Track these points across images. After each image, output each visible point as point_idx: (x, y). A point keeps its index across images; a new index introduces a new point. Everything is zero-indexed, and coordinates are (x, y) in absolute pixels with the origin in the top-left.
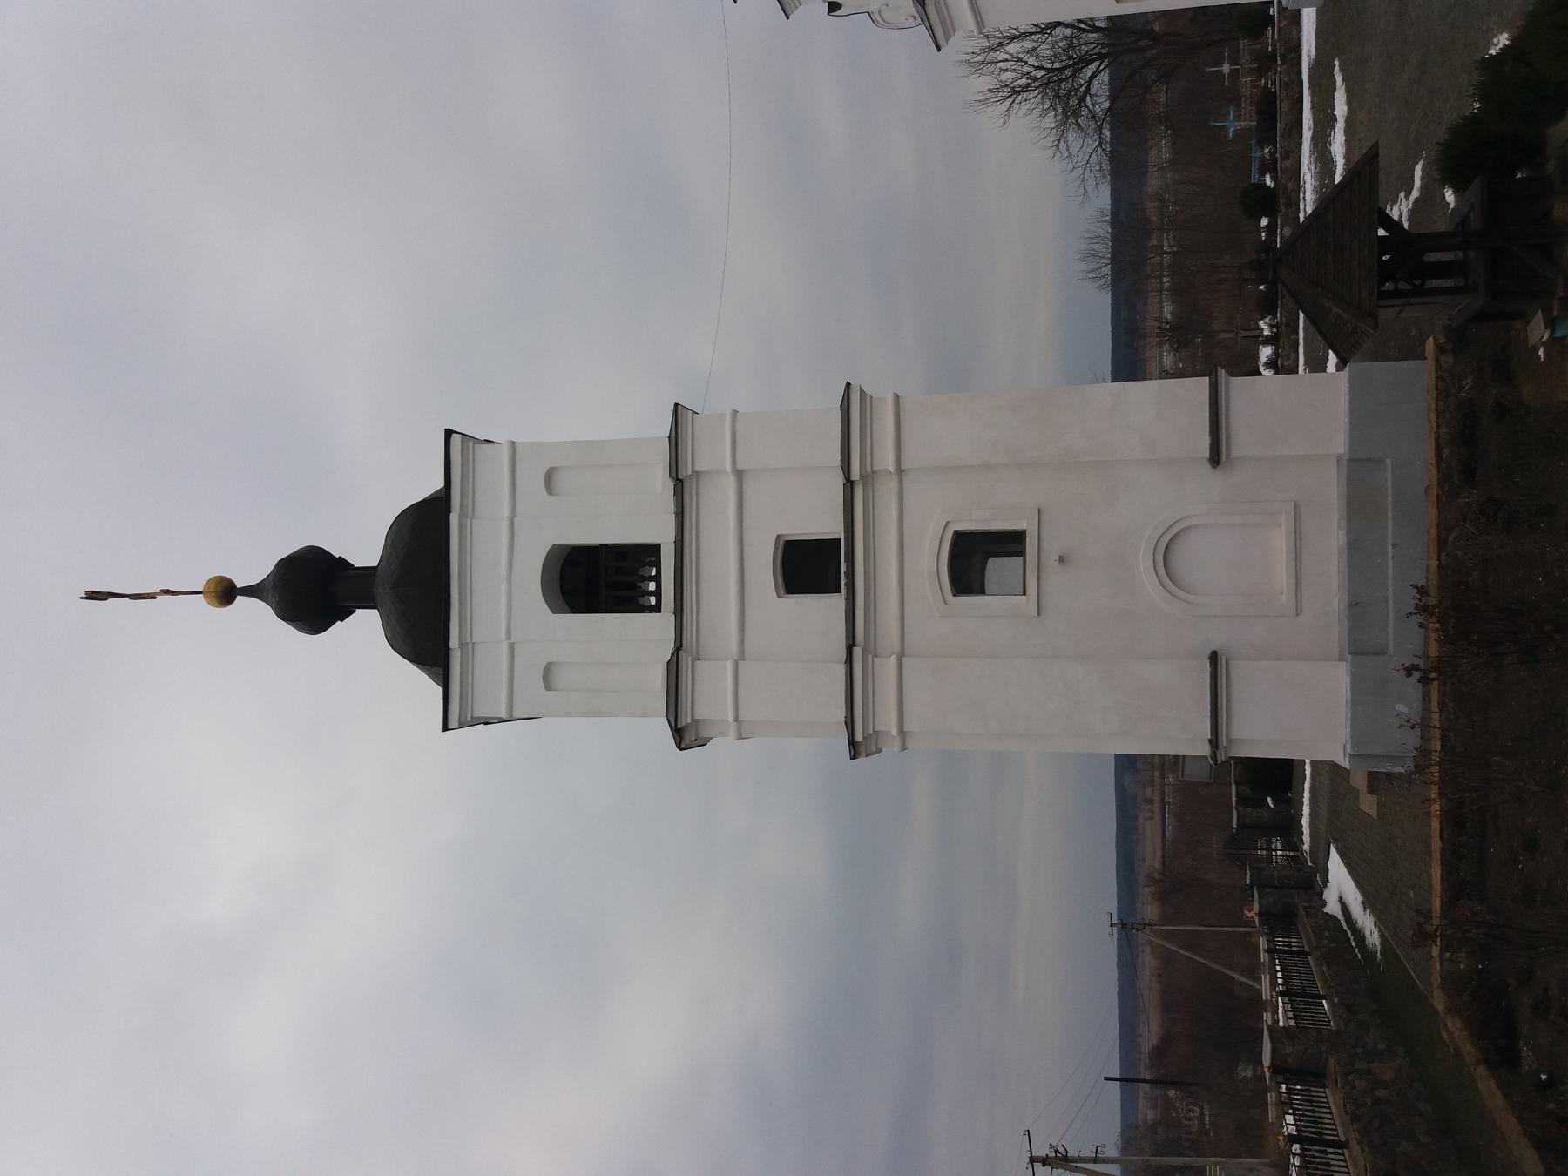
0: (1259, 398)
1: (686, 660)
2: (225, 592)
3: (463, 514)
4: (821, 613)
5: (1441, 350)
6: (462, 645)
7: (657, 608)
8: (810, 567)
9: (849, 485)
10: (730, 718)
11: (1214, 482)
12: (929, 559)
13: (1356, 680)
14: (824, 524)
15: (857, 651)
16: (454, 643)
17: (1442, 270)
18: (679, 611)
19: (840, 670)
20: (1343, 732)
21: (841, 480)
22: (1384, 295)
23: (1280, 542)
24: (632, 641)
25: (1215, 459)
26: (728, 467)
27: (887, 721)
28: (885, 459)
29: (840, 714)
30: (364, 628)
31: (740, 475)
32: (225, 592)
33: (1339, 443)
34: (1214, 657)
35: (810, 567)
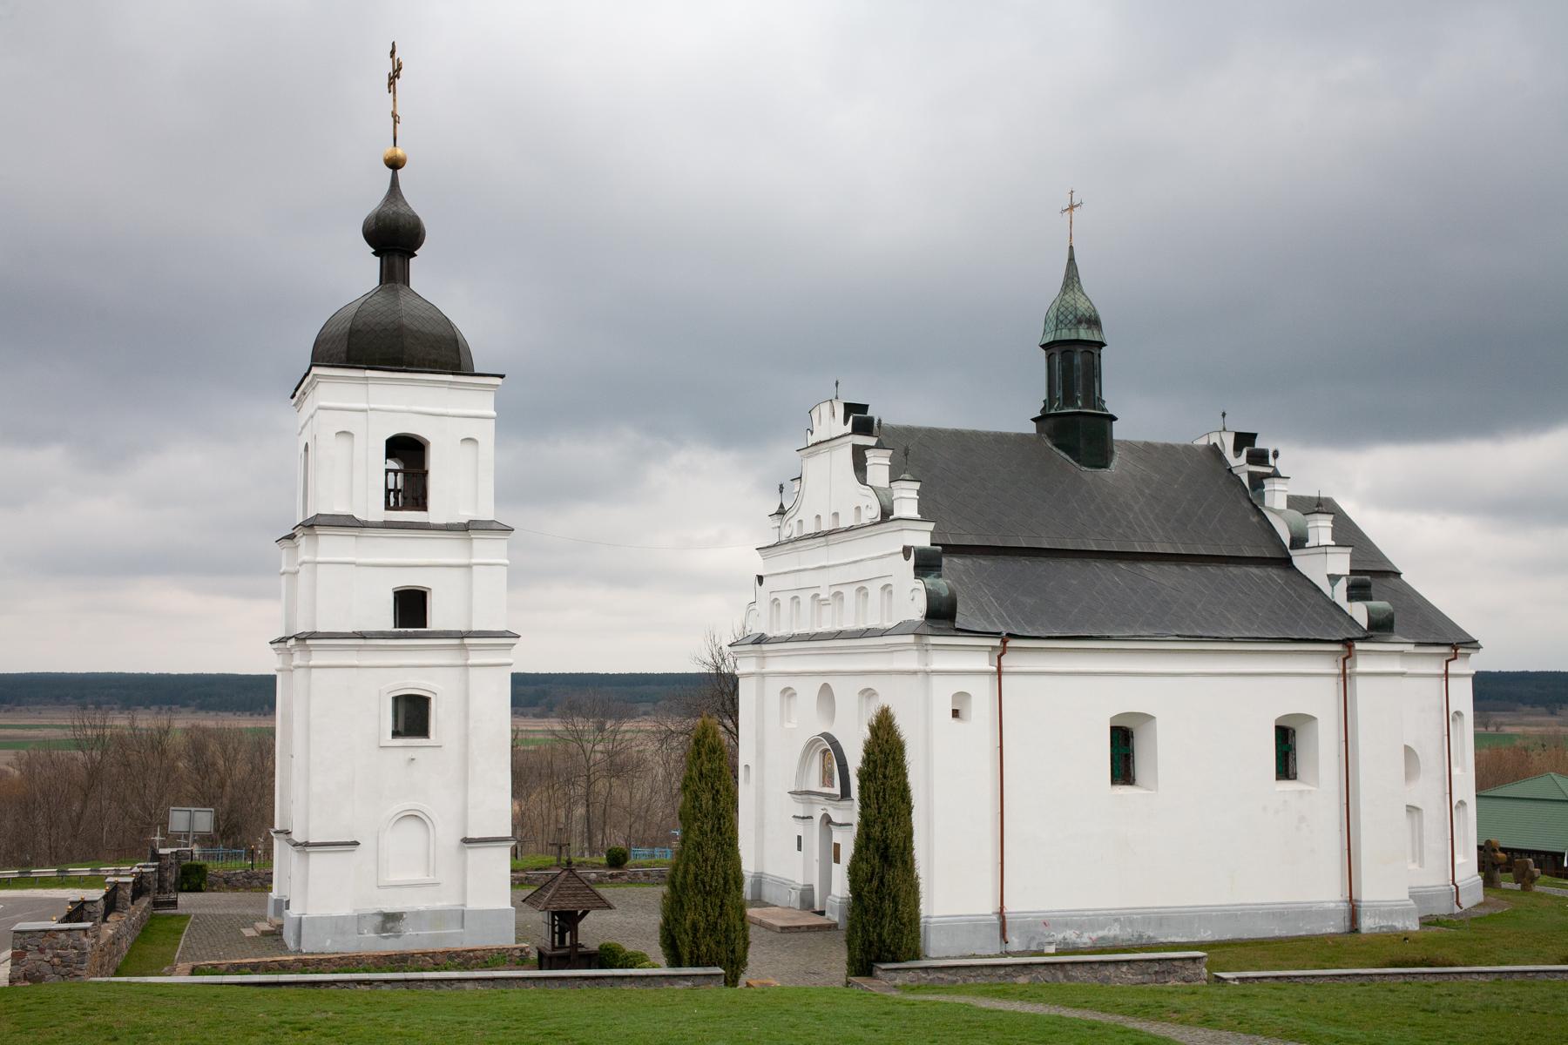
0: (499, 863)
1: (356, 532)
2: (395, 164)
3: (451, 383)
5: (522, 950)
6: (367, 378)
7: (388, 507)
8: (411, 607)
9: (462, 635)
10: (319, 559)
11: (455, 840)
12: (413, 684)
13: (344, 918)
14: (437, 617)
15: (362, 642)
16: (369, 373)
17: (562, 940)
18: (388, 525)
19: (349, 630)
20: (313, 912)
21: (463, 629)
22: (554, 914)
23: (419, 876)
24: (363, 483)
25: (466, 841)
26: (474, 561)
27: (318, 658)
28: (475, 658)
29: (320, 629)
30: (365, 270)
31: (469, 566)
32: (395, 164)
33: (472, 905)
34: (356, 843)
35: (411, 607)
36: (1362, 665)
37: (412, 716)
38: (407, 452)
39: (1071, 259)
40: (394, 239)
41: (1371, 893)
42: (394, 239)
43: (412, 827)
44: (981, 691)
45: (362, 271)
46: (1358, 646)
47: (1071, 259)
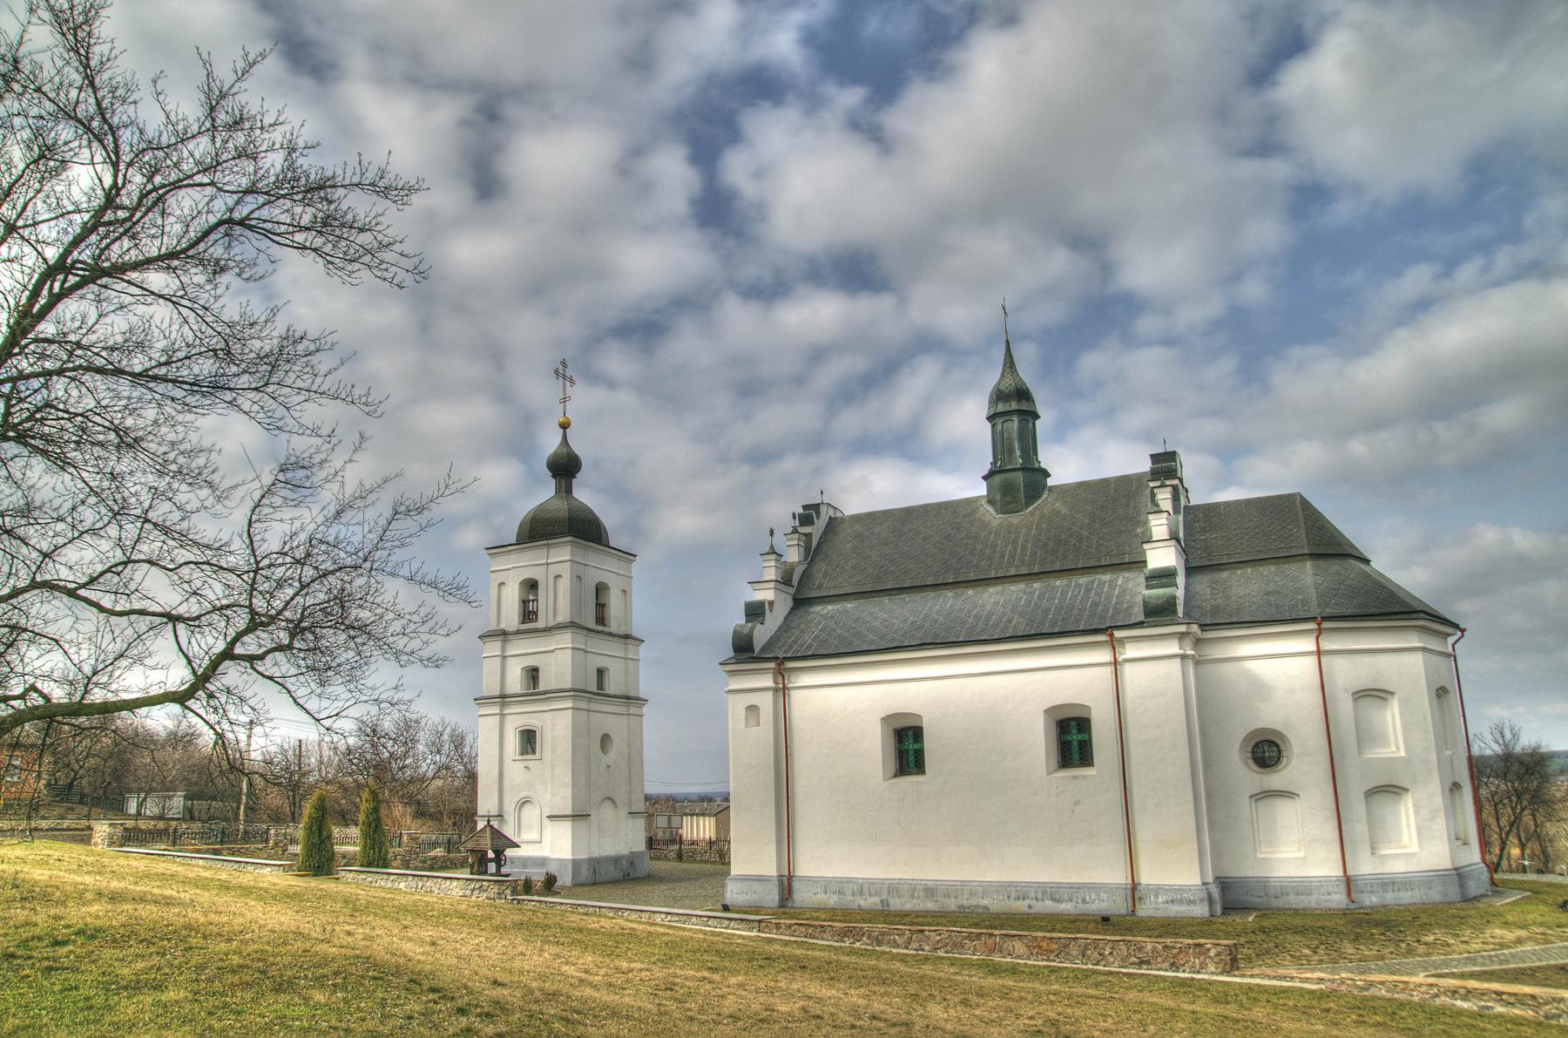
2: (565, 426)
4: (515, 682)
8: (533, 674)
18: (518, 632)
32: (565, 426)
36: (1131, 651)
37: (529, 739)
38: (531, 586)
39: (1008, 349)
40: (565, 468)
41: (1147, 877)
42: (565, 468)
43: (527, 808)
44: (765, 702)
45: (545, 492)
46: (1118, 634)
47: (1008, 349)
